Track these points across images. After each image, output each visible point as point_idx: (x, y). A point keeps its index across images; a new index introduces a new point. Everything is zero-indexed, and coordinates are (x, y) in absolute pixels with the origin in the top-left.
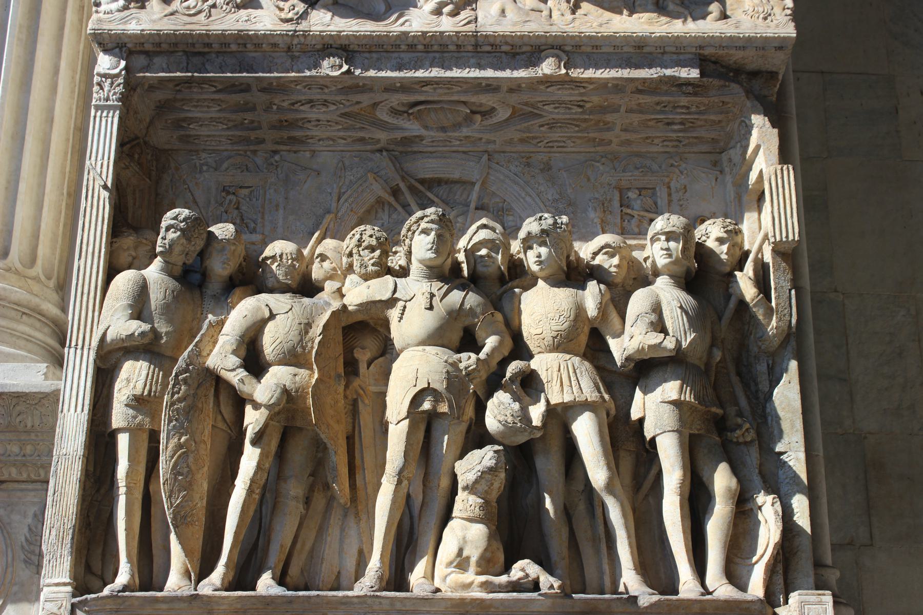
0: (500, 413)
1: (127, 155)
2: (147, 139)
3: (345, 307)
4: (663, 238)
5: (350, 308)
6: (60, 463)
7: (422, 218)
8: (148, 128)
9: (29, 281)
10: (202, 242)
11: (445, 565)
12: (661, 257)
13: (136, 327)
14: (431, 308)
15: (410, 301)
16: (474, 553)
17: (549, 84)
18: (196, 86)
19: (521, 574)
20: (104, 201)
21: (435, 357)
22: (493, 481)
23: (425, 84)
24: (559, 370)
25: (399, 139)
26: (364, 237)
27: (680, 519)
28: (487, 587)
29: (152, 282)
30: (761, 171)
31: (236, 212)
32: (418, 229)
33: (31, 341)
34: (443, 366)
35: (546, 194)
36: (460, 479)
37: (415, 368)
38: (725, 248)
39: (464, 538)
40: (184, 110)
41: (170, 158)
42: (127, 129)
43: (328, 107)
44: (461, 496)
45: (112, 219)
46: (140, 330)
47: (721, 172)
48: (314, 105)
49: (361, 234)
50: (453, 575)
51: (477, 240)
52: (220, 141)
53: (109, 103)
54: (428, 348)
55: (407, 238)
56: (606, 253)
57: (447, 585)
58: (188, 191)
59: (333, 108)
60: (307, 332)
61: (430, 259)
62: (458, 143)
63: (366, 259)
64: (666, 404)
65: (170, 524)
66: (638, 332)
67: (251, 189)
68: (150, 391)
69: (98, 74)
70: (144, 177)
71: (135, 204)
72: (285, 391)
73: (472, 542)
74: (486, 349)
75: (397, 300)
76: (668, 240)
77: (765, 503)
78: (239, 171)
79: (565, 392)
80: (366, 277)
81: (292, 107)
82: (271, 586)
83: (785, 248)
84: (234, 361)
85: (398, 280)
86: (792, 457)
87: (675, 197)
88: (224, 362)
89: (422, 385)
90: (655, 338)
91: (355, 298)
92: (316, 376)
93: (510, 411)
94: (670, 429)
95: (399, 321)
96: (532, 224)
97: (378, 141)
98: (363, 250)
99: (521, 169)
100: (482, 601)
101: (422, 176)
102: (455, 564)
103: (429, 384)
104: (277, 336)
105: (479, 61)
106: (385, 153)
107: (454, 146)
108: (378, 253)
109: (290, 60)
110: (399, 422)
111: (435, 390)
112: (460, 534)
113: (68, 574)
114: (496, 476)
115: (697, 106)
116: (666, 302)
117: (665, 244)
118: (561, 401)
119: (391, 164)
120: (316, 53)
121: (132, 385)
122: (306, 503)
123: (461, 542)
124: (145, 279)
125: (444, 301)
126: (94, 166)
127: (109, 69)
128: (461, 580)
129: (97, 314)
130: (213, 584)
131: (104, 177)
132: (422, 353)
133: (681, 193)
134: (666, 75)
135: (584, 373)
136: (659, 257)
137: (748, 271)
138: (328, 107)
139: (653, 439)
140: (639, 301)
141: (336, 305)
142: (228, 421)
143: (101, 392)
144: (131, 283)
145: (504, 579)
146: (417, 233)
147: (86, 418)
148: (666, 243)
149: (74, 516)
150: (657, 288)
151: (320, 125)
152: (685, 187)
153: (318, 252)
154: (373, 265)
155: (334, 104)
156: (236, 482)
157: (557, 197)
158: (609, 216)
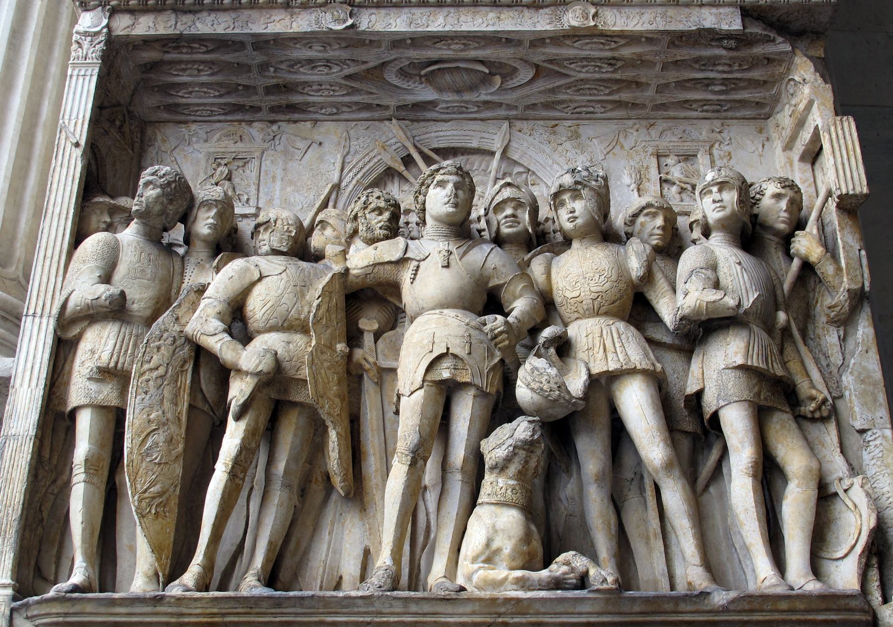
0: (534, 380)
1: (108, 120)
2: (131, 108)
3: (347, 270)
4: (715, 189)
5: (353, 272)
6: (7, 445)
7: (438, 170)
8: (133, 95)
9: (7, 282)
10: (185, 203)
11: (471, 560)
12: (714, 210)
13: (102, 291)
14: (447, 266)
15: (424, 260)
16: (507, 545)
17: (577, 39)
18: (185, 46)
19: (565, 568)
20: (76, 160)
21: (454, 319)
22: (528, 458)
23: (437, 40)
24: (601, 336)
25: (410, 106)
26: (371, 199)
27: (753, 504)
28: (522, 583)
29: (125, 244)
30: (816, 128)
31: (227, 183)
32: (432, 182)
33: (6, 346)
34: (465, 330)
35: (576, 162)
36: (487, 460)
37: (431, 331)
38: (783, 204)
39: (494, 526)
40: (171, 74)
41: (157, 131)
42: (108, 93)
43: (330, 68)
44: (488, 478)
45: (84, 179)
46: (108, 293)
47: (768, 139)
48: (316, 67)
49: (367, 196)
50: (481, 572)
51: (501, 200)
52: (212, 111)
53: (88, 61)
54: (446, 311)
55: (420, 194)
56: (647, 215)
57: (474, 584)
58: (175, 163)
59: (336, 69)
60: (303, 295)
61: (449, 215)
62: (476, 109)
63: (374, 222)
64: (730, 371)
65: (134, 513)
66: (694, 288)
67: (244, 161)
68: (117, 363)
69: (77, 33)
70: (126, 147)
71: (115, 175)
72: (278, 365)
73: (503, 530)
74: (514, 313)
75: (409, 259)
77: (852, 485)
78: (232, 142)
79: (609, 359)
80: (372, 241)
81: (291, 70)
82: (255, 587)
83: (851, 204)
84: (216, 324)
85: (410, 242)
86: (877, 435)
88: (205, 327)
89: (440, 350)
90: (712, 296)
91: (361, 260)
92: (314, 343)
93: (546, 377)
94: (737, 399)
95: (412, 283)
96: (564, 176)
97: (387, 108)
98: (370, 213)
100: (518, 600)
101: (436, 146)
102: (483, 558)
103: (448, 349)
104: (268, 298)
105: (498, 15)
106: (394, 121)
107: (471, 113)
108: (386, 215)
109: (289, 17)
110: (412, 393)
111: (455, 356)
112: (488, 522)
113: (9, 573)
114: (532, 452)
115: (740, 65)
116: (722, 258)
117: (717, 197)
118: (605, 369)
119: (401, 133)
120: (318, 9)
121: (96, 356)
122: (302, 496)
123: (491, 531)
124: (117, 240)
125: (465, 259)
126: (67, 124)
127: (88, 27)
128: (491, 577)
129: (60, 279)
130: (185, 585)
131: (77, 136)
132: (439, 316)
133: (725, 160)
134: (706, 27)
135: (630, 339)
136: (711, 211)
137: (811, 230)
138: (330, 68)
139: (715, 416)
140: (690, 259)
141: (337, 268)
142: (210, 400)
143: (63, 368)
144: (101, 244)
145: (544, 573)
146: (432, 187)
147: (42, 393)
148: (718, 195)
149: (21, 506)
150: (712, 245)
151: (322, 90)
152: (729, 154)
153: (318, 219)
154: (381, 228)
155: (337, 65)
156: (216, 467)
158: (647, 184)
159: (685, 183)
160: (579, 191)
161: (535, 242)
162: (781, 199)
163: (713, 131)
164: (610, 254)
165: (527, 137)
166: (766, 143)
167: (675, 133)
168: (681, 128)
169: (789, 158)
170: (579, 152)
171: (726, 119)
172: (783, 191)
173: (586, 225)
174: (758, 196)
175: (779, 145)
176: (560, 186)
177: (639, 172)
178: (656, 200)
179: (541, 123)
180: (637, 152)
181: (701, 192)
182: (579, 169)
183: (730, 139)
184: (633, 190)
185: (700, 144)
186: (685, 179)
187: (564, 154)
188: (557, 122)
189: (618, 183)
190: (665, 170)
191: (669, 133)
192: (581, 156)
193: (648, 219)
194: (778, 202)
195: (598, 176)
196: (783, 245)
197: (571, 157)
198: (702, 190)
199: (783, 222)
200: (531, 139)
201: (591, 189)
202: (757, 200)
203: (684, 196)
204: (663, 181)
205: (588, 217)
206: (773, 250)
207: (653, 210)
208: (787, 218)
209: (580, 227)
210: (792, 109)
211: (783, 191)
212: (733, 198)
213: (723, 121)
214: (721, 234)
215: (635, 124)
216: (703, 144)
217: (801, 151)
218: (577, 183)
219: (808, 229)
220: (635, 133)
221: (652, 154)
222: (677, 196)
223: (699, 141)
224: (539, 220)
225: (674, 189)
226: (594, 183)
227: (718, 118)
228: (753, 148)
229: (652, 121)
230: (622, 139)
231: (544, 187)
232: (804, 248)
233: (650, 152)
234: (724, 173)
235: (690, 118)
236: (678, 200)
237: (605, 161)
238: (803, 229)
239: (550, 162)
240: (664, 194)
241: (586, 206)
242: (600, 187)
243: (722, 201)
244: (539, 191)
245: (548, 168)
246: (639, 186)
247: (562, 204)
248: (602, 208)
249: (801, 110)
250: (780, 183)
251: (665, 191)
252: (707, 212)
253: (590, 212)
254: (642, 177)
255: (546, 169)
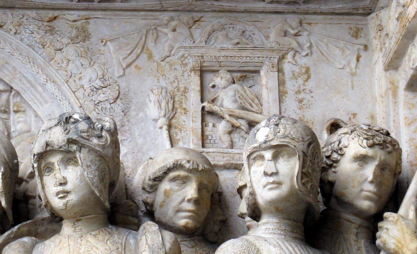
4: (268, 155)
12: (265, 187)
35: (80, 79)
47: (366, 47)
56: (174, 179)
76: (275, 157)
87: (290, 86)
99: (39, 36)
117: (270, 167)
133: (300, 81)
136: (261, 187)
148: (272, 164)
152: (307, 71)
157: (98, 83)
158: (183, 117)
159: (238, 118)
160: (74, 152)
161: (11, 218)
162: (366, 163)
163: (286, 34)
164: (114, 248)
165: (10, 37)
166: (363, 54)
167: (231, 35)
168: (240, 27)
169: (392, 83)
170: (85, 62)
171: (307, 13)
172: (370, 152)
173: (82, 202)
174: (335, 156)
175: (381, 60)
176: (47, 145)
177: (173, 98)
178: (188, 158)
179: (32, 13)
180: (171, 65)
181: (249, 157)
182: (76, 116)
183: (311, 47)
184: (161, 128)
185: (266, 53)
186: (239, 112)
187: (64, 65)
188: (56, 13)
189: (141, 114)
190: (209, 96)
191: (220, 35)
192: (89, 71)
193: (174, 186)
194: (362, 167)
195: (102, 128)
196: (367, 228)
197: (75, 71)
198: (251, 154)
199: (368, 198)
200: (15, 40)
201: (91, 150)
202: (334, 162)
203: (236, 136)
204: (205, 113)
205: (85, 191)
206: (352, 237)
207: (182, 173)
208: (374, 193)
209: (73, 206)
210: (400, 9)
211: (370, 152)
212: (292, 169)
213: (301, 17)
214: (275, 220)
215: (172, 19)
216: (270, 54)
217: (409, 77)
218: (70, 141)
219: (402, 210)
220: (171, 35)
221: (193, 70)
222: (226, 138)
223: (263, 49)
224: (20, 174)
225: (222, 126)
226: (95, 141)
227: (294, 12)
228: (344, 62)
229: (197, 15)
230: (150, 44)
231: (33, 116)
232: (393, 241)
233: (190, 66)
234: (282, 131)
235: (254, 12)
236: (227, 144)
237: (124, 78)
238: (396, 210)
239: (42, 78)
240: (207, 133)
241: (82, 175)
242: (103, 147)
243: (276, 174)
244: (25, 122)
245: (40, 89)
246: (171, 120)
247: (50, 168)
248: (107, 176)
249: (411, 15)
250: (367, 139)
251: (209, 129)
252: (255, 187)
253: (87, 184)
254: (177, 106)
255: (36, 89)
